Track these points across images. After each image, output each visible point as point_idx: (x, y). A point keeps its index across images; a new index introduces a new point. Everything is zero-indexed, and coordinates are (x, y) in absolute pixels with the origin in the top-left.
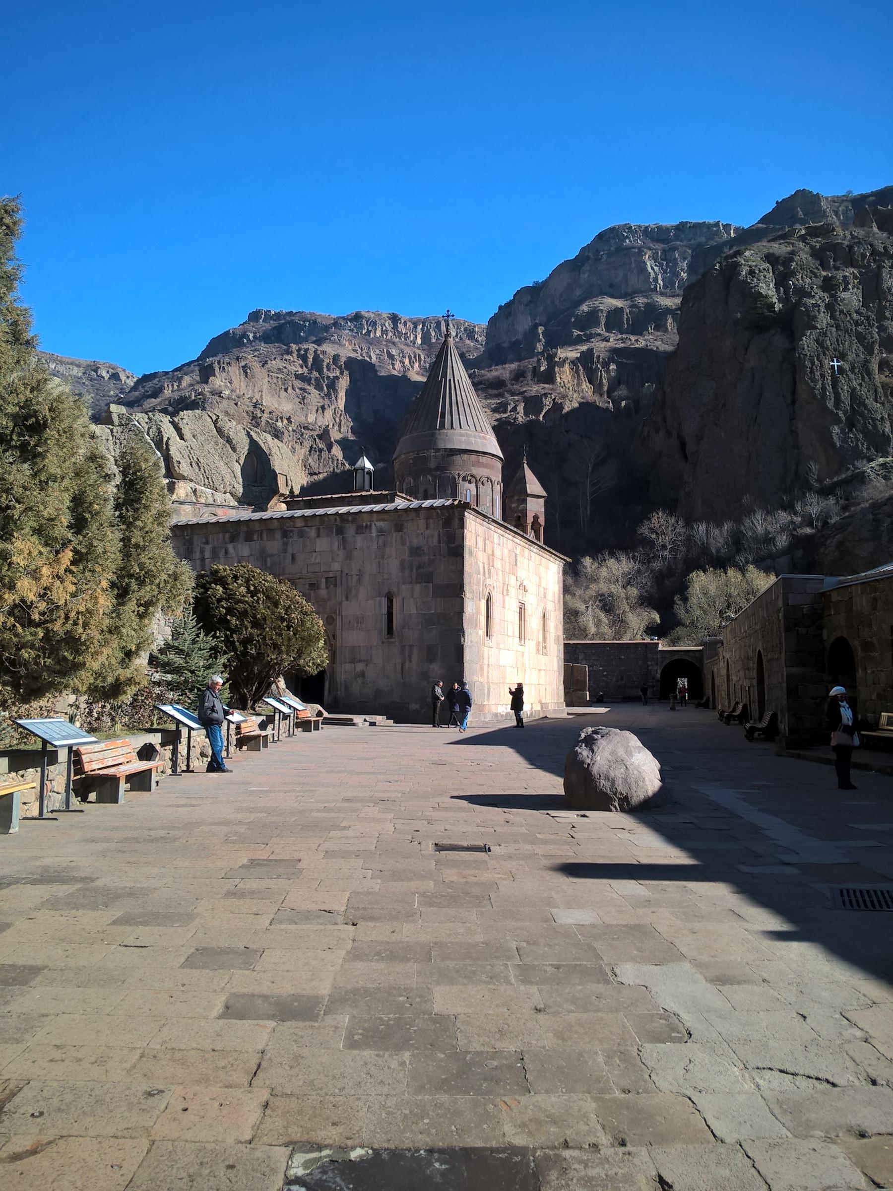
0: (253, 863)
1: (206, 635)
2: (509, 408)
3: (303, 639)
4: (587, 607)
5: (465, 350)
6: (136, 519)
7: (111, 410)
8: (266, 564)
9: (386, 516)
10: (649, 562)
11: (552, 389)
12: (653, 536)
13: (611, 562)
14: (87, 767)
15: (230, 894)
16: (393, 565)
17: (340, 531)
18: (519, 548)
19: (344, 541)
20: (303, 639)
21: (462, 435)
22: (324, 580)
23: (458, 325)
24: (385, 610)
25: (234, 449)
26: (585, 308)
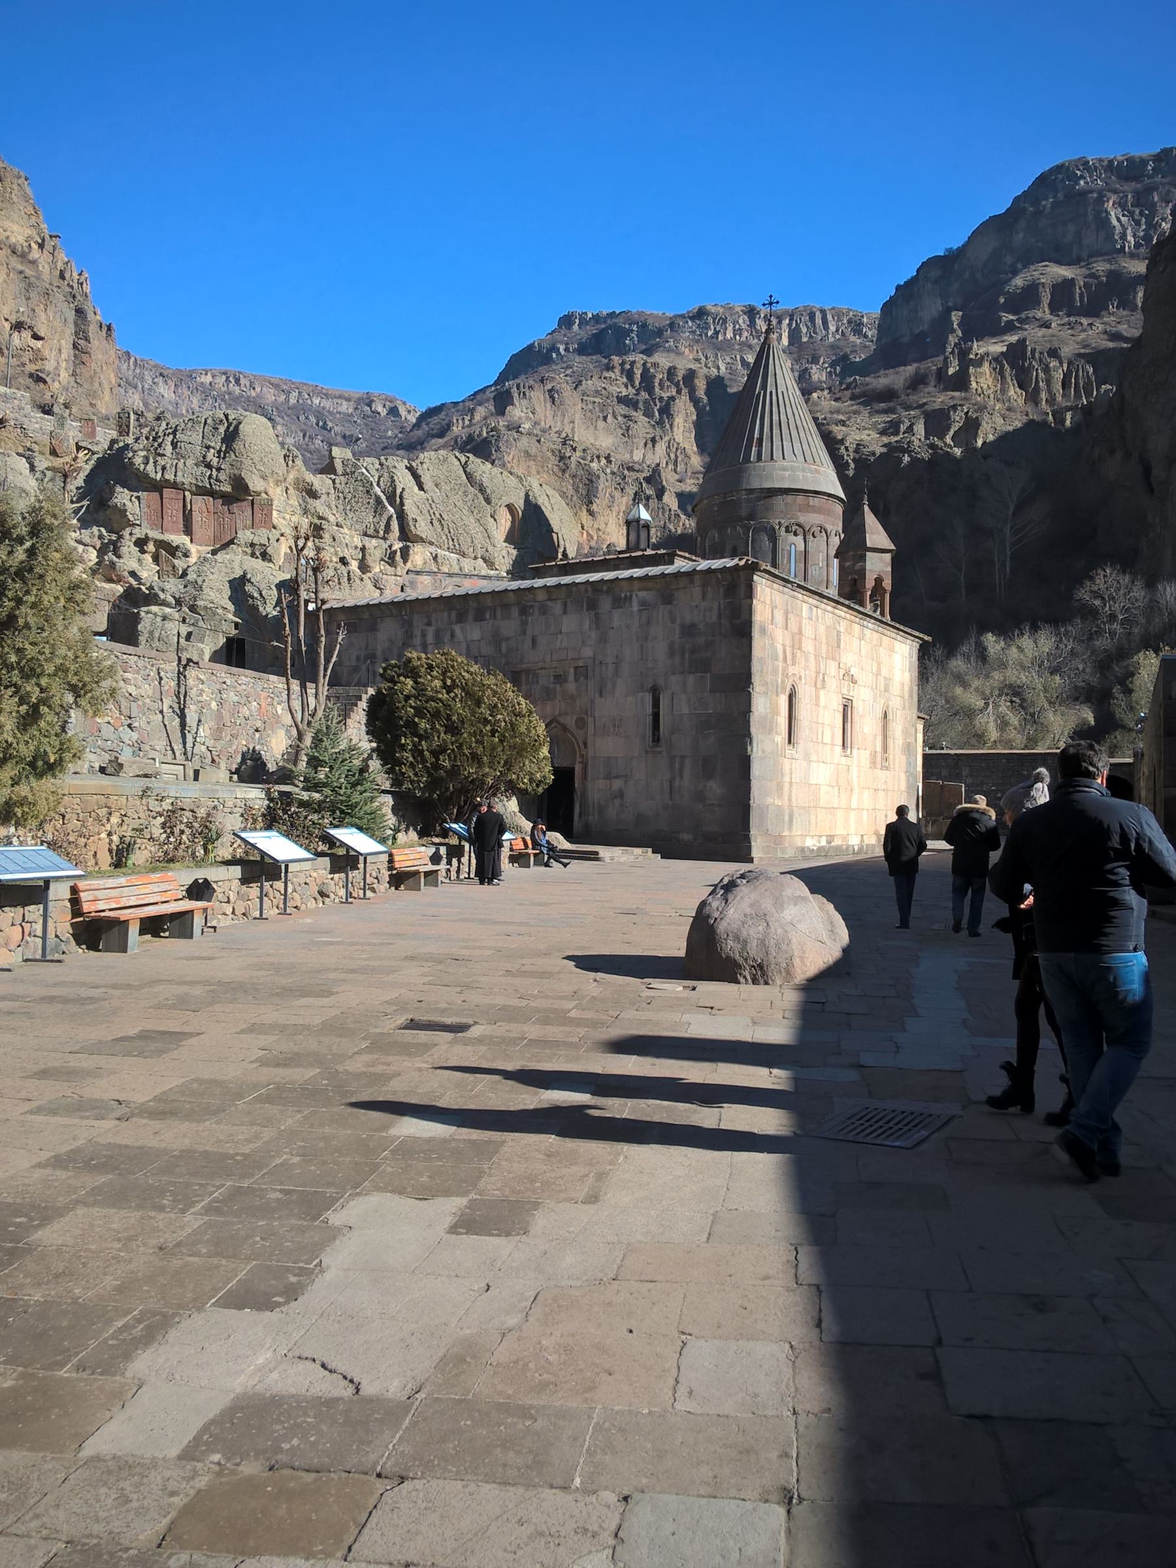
0: (145, 1036)
2: (903, 428)
4: (987, 704)
5: (848, 350)
6: (28, 592)
7: (333, 454)
8: (500, 651)
9: (650, 584)
10: (1090, 639)
11: (965, 399)
12: (1097, 602)
13: (1026, 642)
14: (86, 908)
15: (44, 1074)
16: (659, 651)
17: (593, 605)
18: (844, 623)
19: (597, 615)
21: (784, 469)
22: (572, 671)
23: (839, 315)
25: (488, 501)
26: (1019, 282)
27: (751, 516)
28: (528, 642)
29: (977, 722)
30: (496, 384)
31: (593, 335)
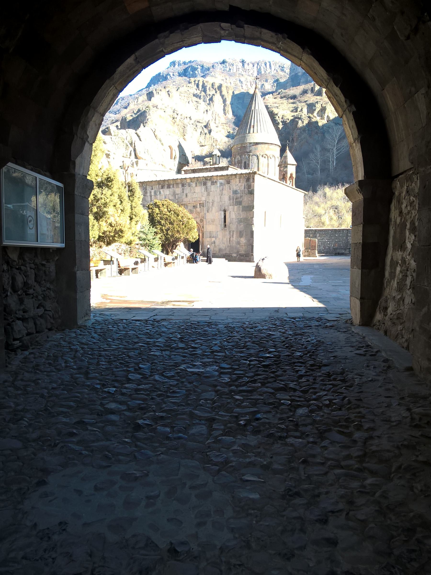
1: (153, 227)
2: (299, 110)
3: (188, 228)
4: (326, 213)
9: (223, 178)
11: (321, 99)
16: (226, 198)
17: (205, 184)
19: (206, 188)
20: (188, 228)
22: (199, 204)
23: (275, 64)
24: (223, 217)
27: (250, 152)
30: (146, 88)
31: (184, 70)
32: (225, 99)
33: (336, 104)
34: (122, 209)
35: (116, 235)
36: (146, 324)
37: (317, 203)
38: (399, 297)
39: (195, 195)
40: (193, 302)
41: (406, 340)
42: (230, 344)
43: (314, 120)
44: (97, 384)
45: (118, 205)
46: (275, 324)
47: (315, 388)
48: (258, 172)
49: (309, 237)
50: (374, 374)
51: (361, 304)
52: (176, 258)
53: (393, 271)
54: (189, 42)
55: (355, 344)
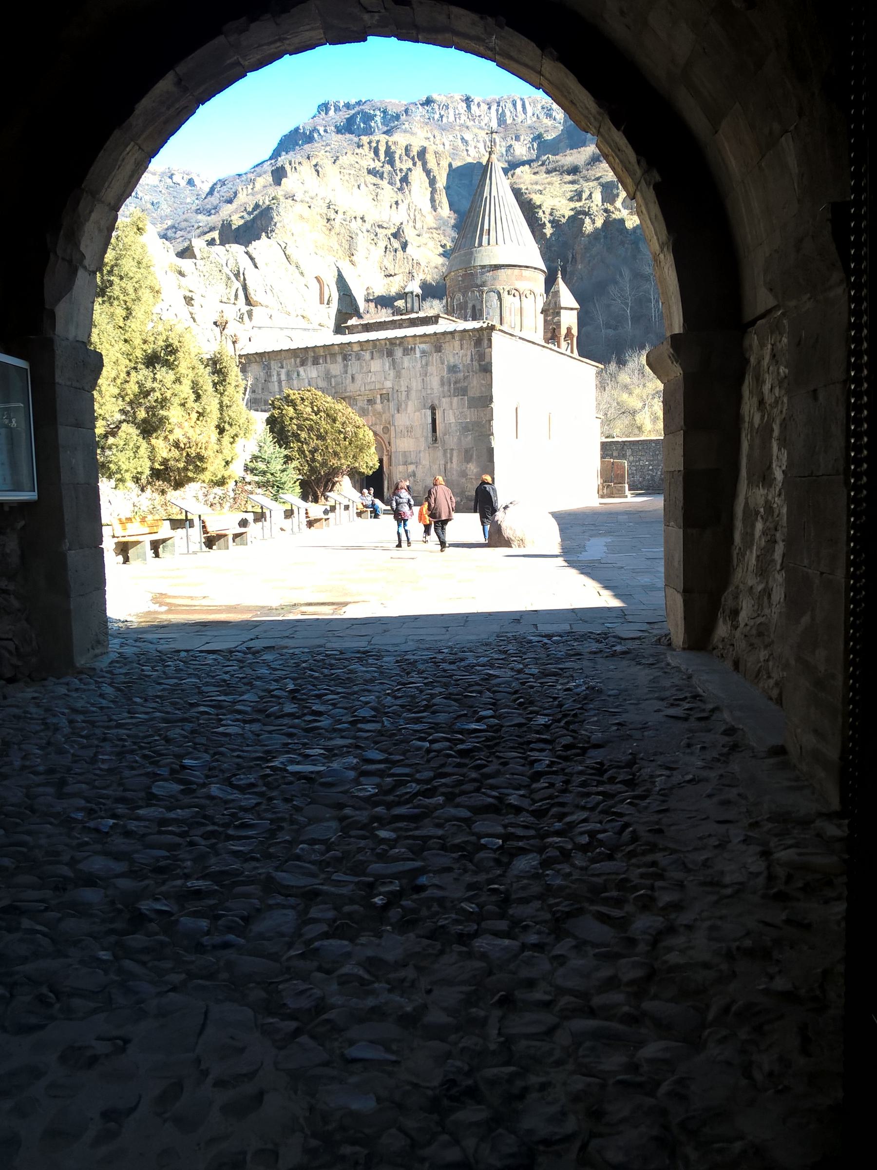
1: (280, 447)
2: (585, 196)
3: (357, 447)
5: (542, 131)
9: (427, 339)
14: (209, 529)
16: (434, 382)
17: (390, 354)
19: (393, 360)
20: (357, 447)
22: (379, 396)
24: (430, 421)
27: (484, 284)
28: (349, 379)
29: (637, 418)
30: (271, 159)
31: (348, 119)
32: (434, 177)
33: (620, 170)
34: (201, 411)
35: (191, 467)
36: (229, 660)
37: (626, 387)
38: (760, 587)
39: (371, 378)
40: (345, 604)
41: (777, 684)
42: (399, 702)
43: (616, 216)
44: (79, 809)
45: (190, 404)
46: (505, 652)
47: (562, 805)
48: (498, 326)
49: (612, 457)
50: (700, 763)
51: (686, 603)
52: (333, 509)
53: (749, 531)
54: (296, 40)
55: (668, 693)
